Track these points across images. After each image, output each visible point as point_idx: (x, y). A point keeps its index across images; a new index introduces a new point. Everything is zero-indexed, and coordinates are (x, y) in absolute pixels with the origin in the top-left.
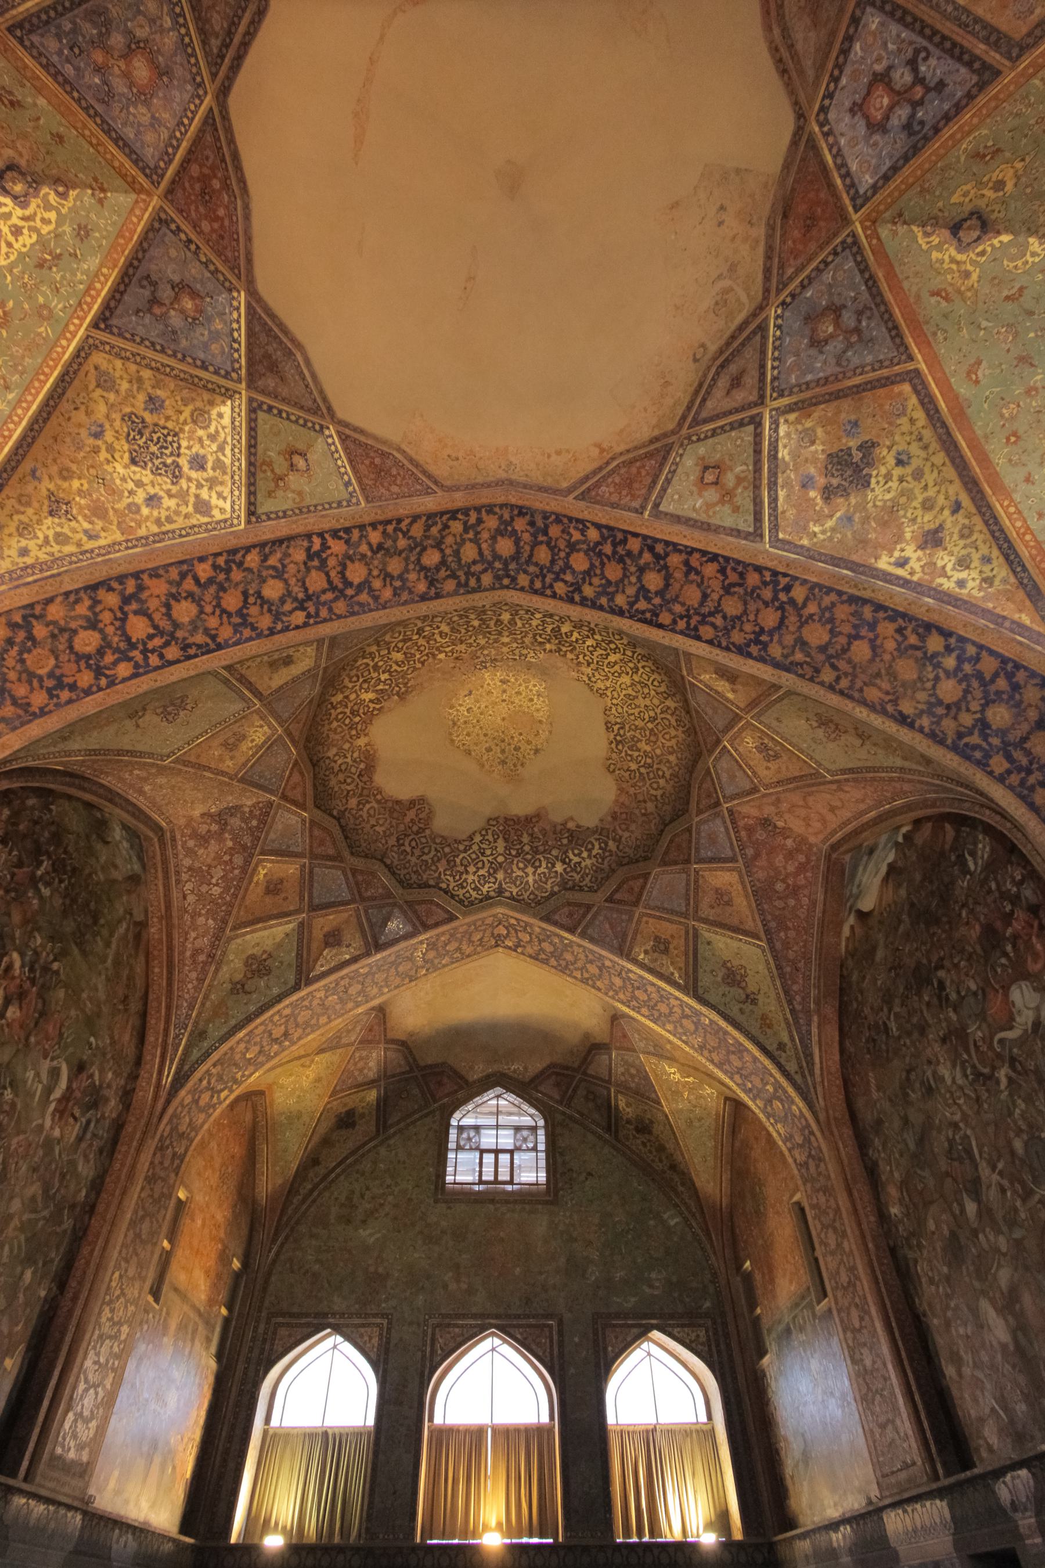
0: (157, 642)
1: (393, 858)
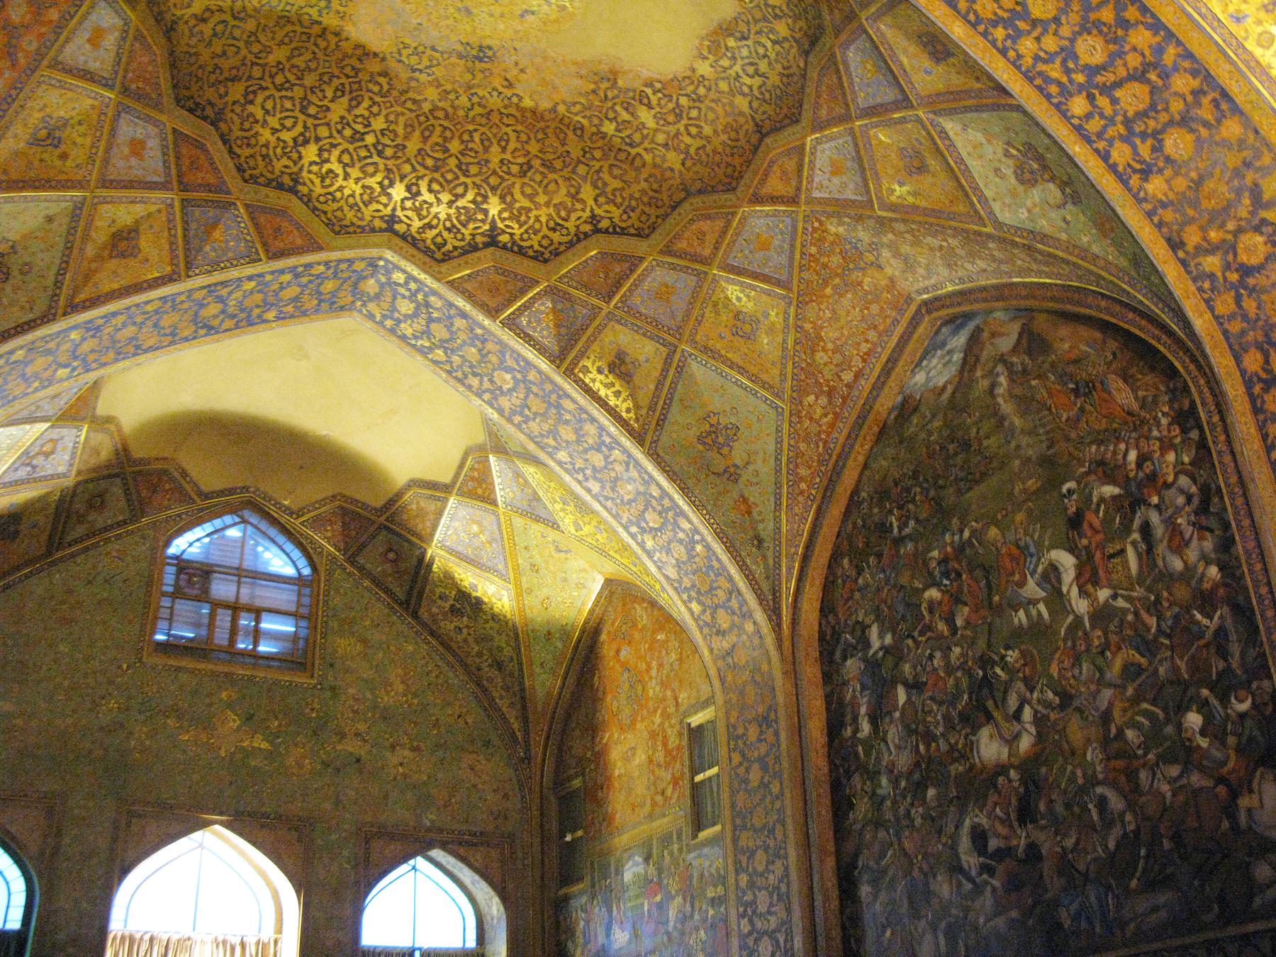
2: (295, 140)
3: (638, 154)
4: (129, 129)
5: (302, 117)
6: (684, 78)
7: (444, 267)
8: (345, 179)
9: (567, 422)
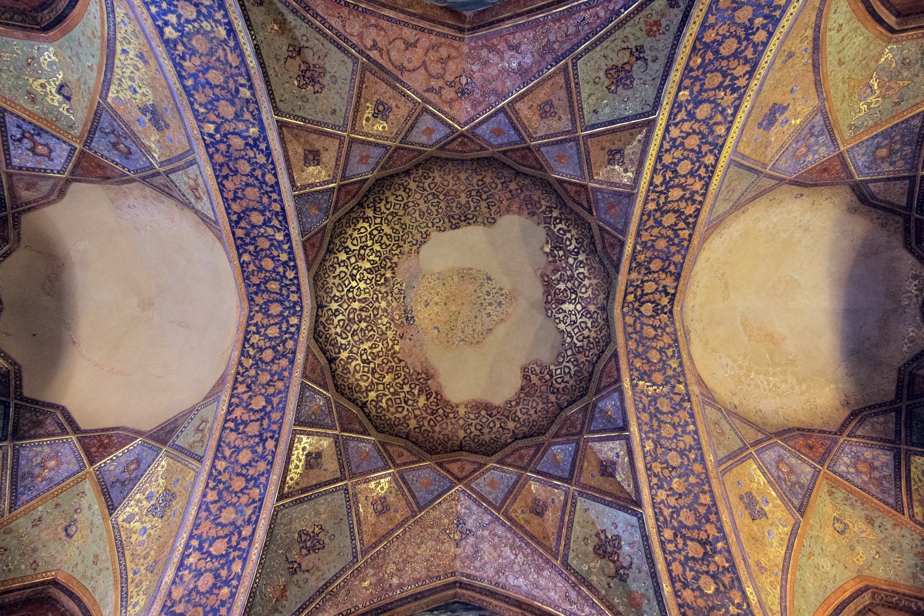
0: (235, 538)
1: (564, 399)
2: (348, 247)
3: (403, 408)
5: (357, 248)
7: (313, 341)
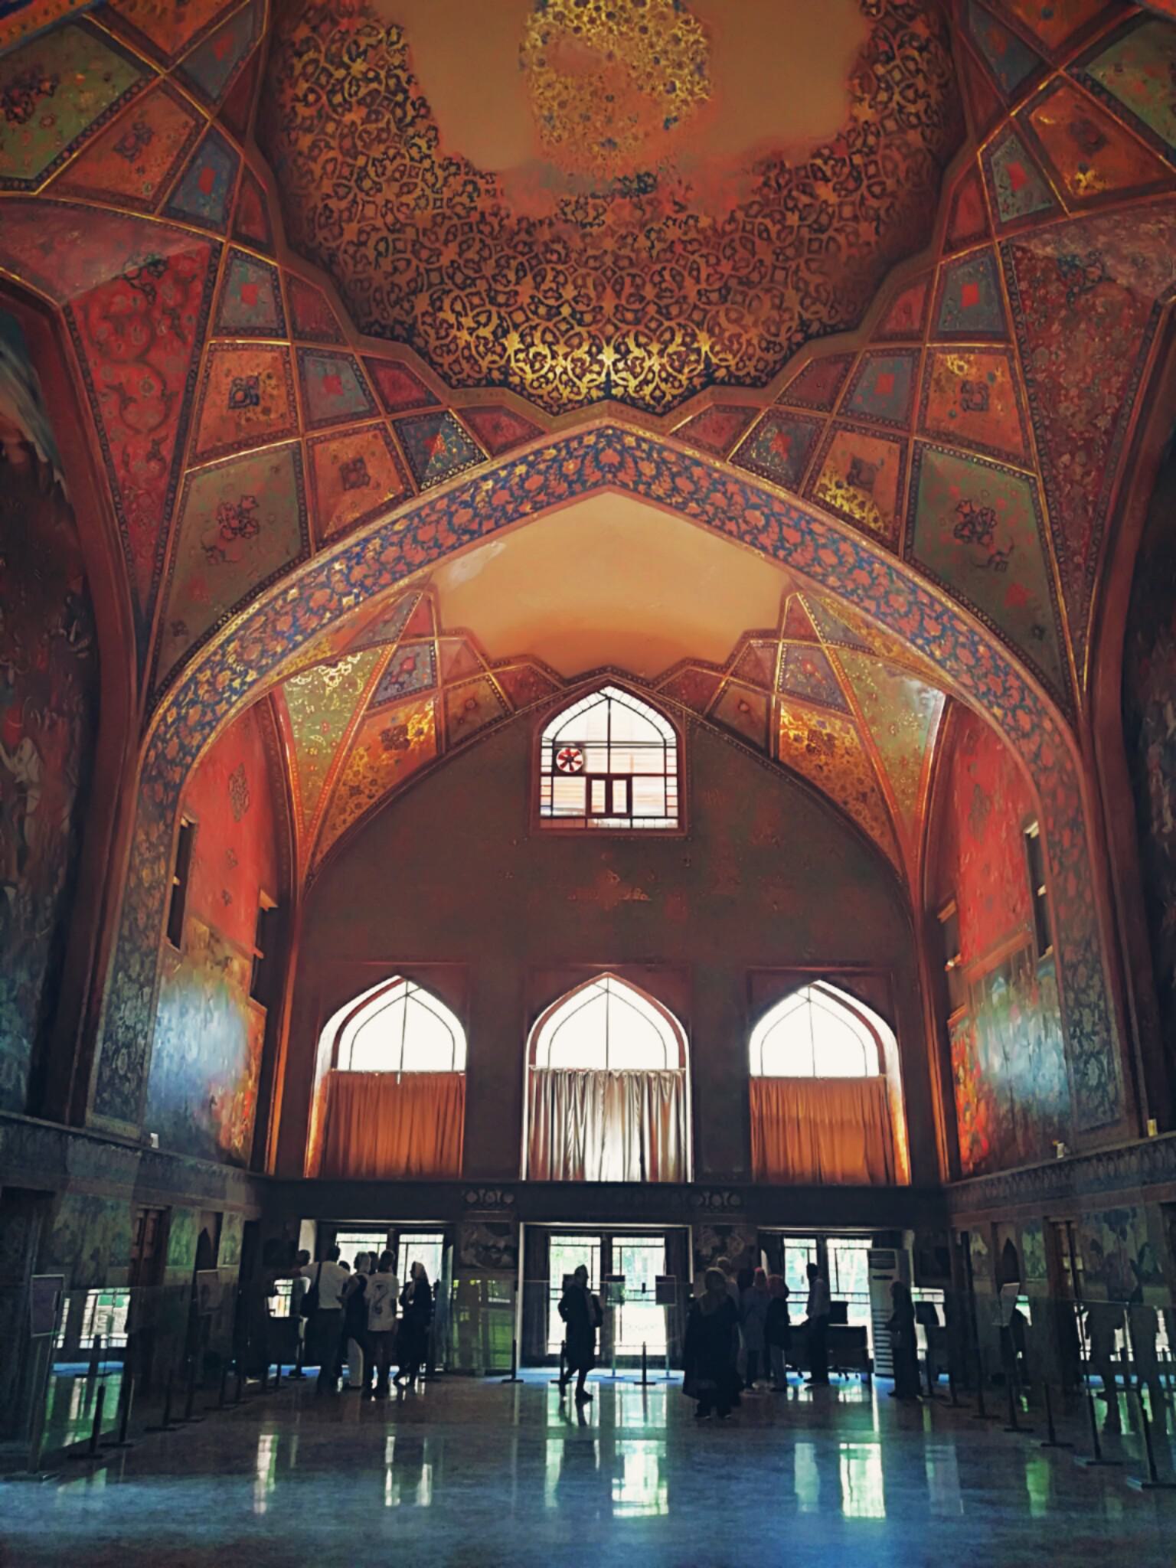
3: (831, 239)
4: (315, 370)
5: (494, 310)
6: (849, 132)
8: (553, 358)
9: (824, 546)
